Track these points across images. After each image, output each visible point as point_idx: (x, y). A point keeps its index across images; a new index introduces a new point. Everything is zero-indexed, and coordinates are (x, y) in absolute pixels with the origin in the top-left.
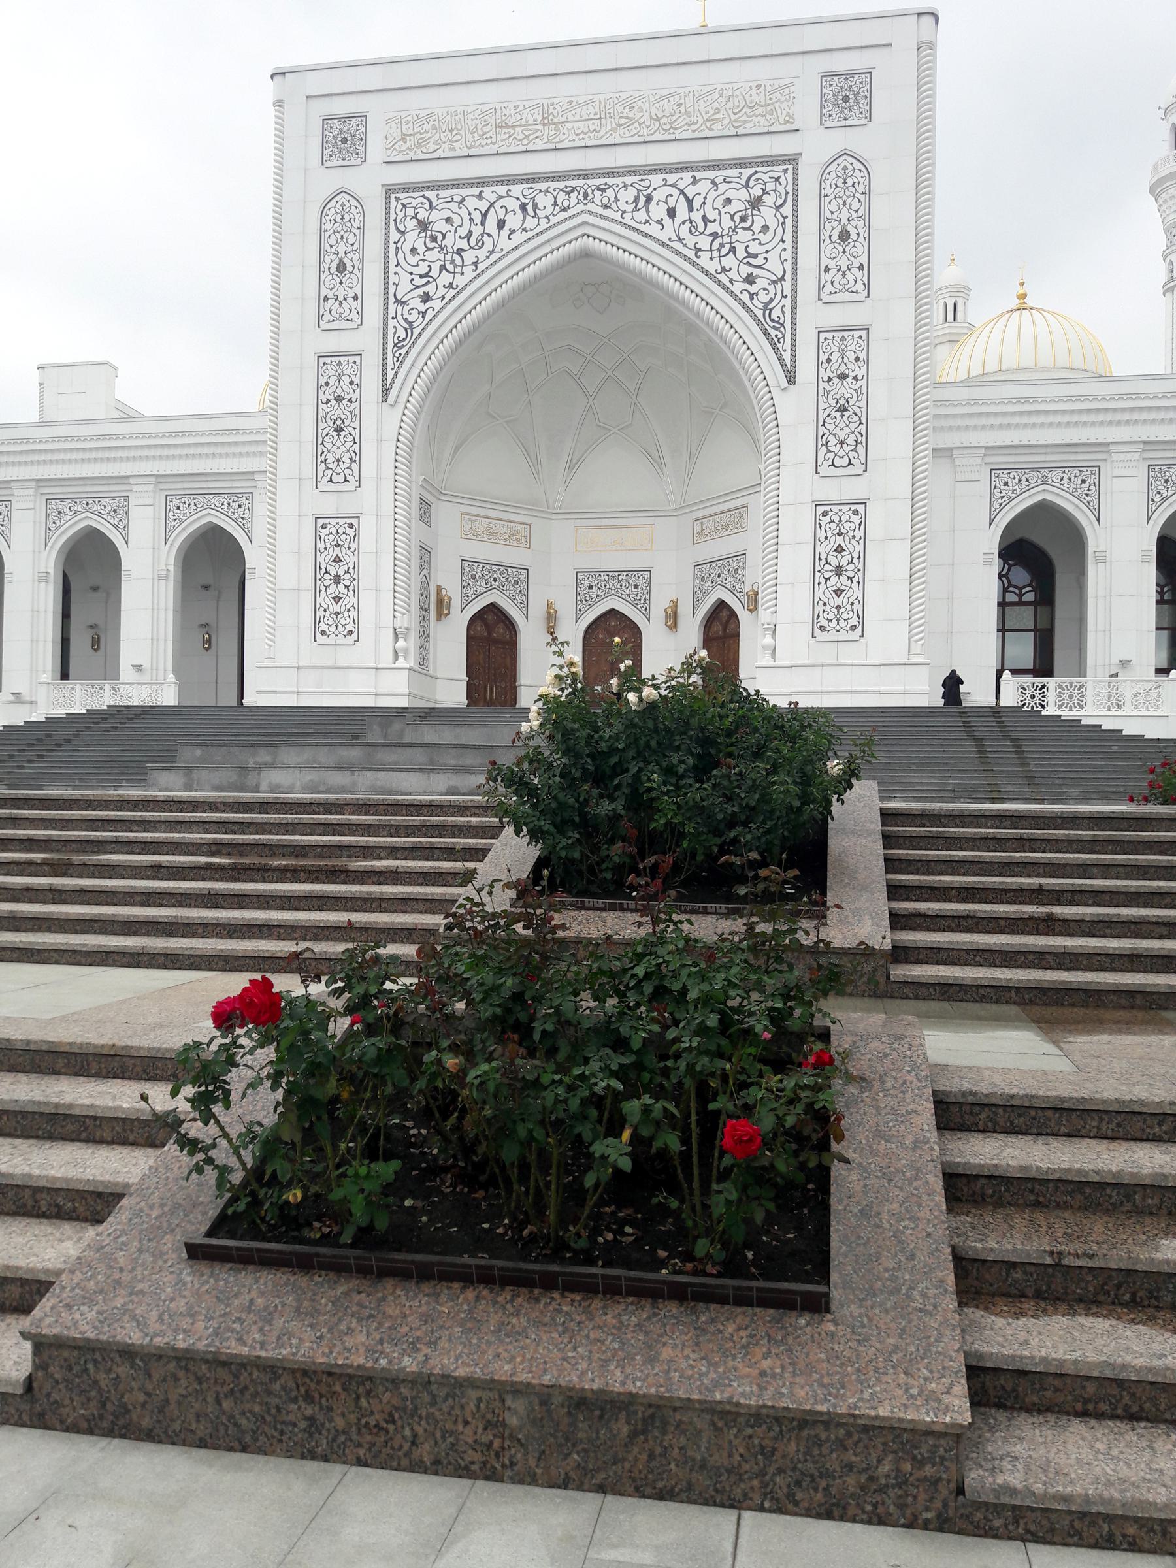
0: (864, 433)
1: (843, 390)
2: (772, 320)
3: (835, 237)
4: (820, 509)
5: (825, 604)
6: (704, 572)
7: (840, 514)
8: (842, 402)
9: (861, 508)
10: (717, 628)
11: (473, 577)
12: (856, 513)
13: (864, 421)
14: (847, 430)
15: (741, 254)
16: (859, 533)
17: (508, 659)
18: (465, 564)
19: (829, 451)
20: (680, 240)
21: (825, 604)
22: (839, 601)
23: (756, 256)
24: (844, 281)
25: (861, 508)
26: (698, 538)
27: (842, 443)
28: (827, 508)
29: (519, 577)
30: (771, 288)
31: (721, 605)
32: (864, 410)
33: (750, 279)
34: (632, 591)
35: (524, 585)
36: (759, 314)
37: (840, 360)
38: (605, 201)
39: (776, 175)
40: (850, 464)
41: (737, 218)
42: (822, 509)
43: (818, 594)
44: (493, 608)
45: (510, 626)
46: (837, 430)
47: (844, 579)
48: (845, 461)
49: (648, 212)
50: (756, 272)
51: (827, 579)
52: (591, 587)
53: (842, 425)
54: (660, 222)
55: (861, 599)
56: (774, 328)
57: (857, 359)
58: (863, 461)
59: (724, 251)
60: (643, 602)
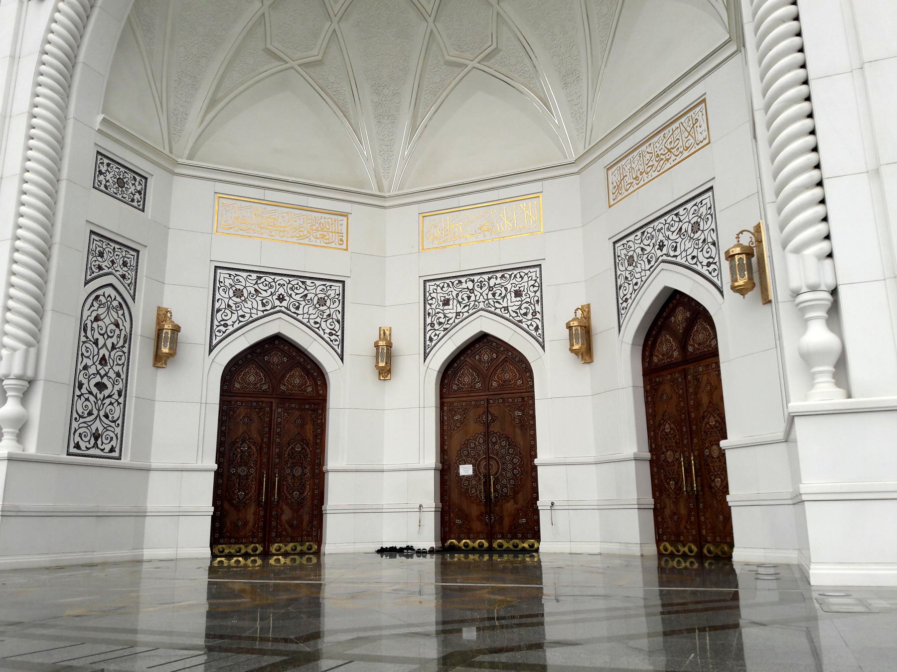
6: (630, 250)
10: (668, 346)
11: (238, 293)
17: (309, 427)
18: (222, 275)
26: (616, 193)
29: (328, 296)
31: (673, 300)
34: (512, 302)
35: (337, 306)
44: (277, 341)
45: (315, 374)
52: (446, 302)
60: (532, 318)
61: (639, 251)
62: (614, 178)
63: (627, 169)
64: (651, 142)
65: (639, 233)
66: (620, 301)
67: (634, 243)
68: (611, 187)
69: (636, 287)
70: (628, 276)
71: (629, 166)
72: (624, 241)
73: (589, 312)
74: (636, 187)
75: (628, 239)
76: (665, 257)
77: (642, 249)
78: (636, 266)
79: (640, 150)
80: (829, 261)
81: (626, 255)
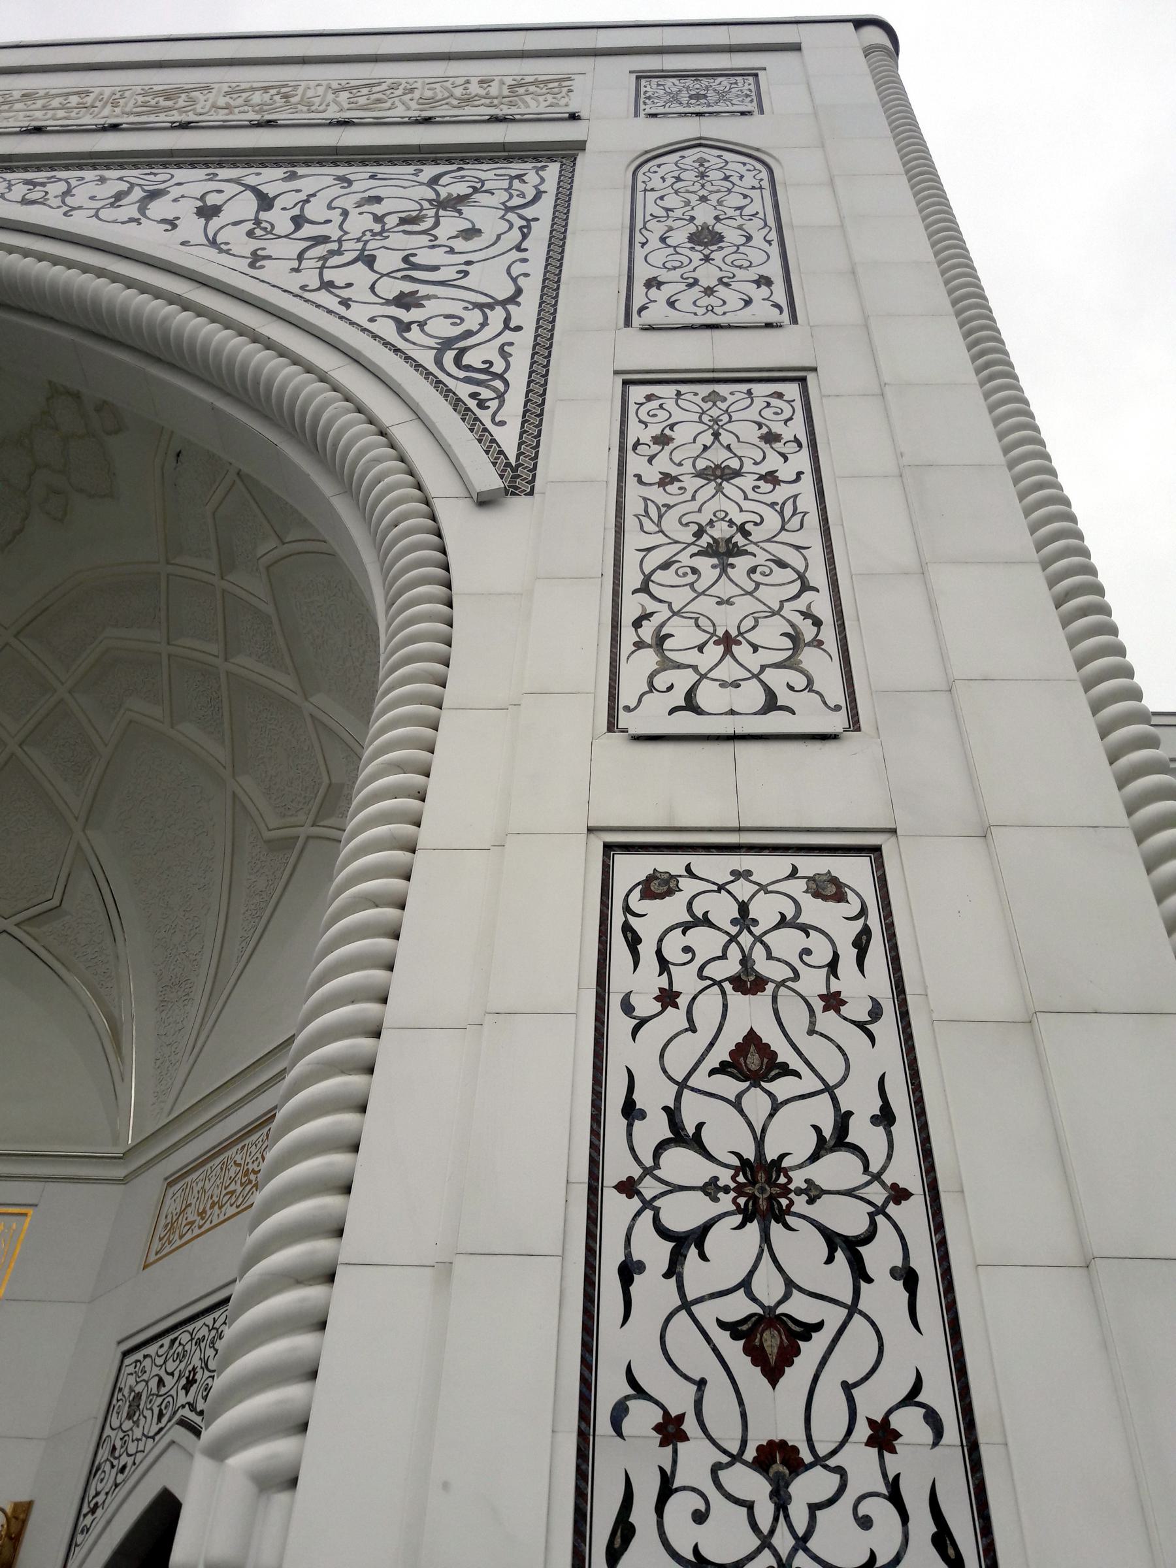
0: (823, 610)
1: (720, 503)
2: (468, 368)
3: (679, 237)
4: (631, 870)
5: (671, 1431)
7: (743, 890)
8: (721, 531)
9: (855, 873)
12: (830, 890)
13: (817, 576)
14: (746, 605)
15: (388, 261)
16: (864, 985)
19: (667, 664)
20: (213, 243)
21: (671, 1431)
22: (777, 1413)
23: (435, 268)
24: (706, 301)
25: (855, 873)
27: (728, 642)
28: (673, 864)
30: (473, 319)
32: (816, 554)
33: (405, 301)
36: (427, 358)
37: (707, 438)
38: (36, 195)
39: (514, 173)
40: (771, 704)
41: (392, 221)
42: (638, 860)
43: (624, 1345)
46: (705, 605)
47: (799, 1248)
48: (753, 696)
49: (142, 210)
50: (424, 290)
51: (686, 1243)
53: (725, 589)
54: (172, 224)
55: (939, 1394)
56: (468, 380)
57: (771, 438)
58: (836, 695)
59: (335, 260)
61: (153, 1383)
62: (171, 1207)
63: (195, 1192)
64: (246, 1142)
65: (166, 1341)
66: (85, 1510)
67: (153, 1362)
68: (162, 1222)
69: (120, 1478)
70: (118, 1444)
71: (201, 1184)
72: (139, 1355)
73: (24, 1523)
74: (197, 1231)
75: (145, 1351)
76: (186, 1412)
77: (161, 1382)
78: (136, 1423)
79: (226, 1155)
80: (282, 1498)
81: (132, 1390)
